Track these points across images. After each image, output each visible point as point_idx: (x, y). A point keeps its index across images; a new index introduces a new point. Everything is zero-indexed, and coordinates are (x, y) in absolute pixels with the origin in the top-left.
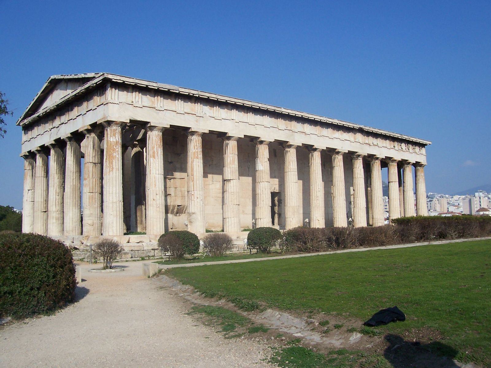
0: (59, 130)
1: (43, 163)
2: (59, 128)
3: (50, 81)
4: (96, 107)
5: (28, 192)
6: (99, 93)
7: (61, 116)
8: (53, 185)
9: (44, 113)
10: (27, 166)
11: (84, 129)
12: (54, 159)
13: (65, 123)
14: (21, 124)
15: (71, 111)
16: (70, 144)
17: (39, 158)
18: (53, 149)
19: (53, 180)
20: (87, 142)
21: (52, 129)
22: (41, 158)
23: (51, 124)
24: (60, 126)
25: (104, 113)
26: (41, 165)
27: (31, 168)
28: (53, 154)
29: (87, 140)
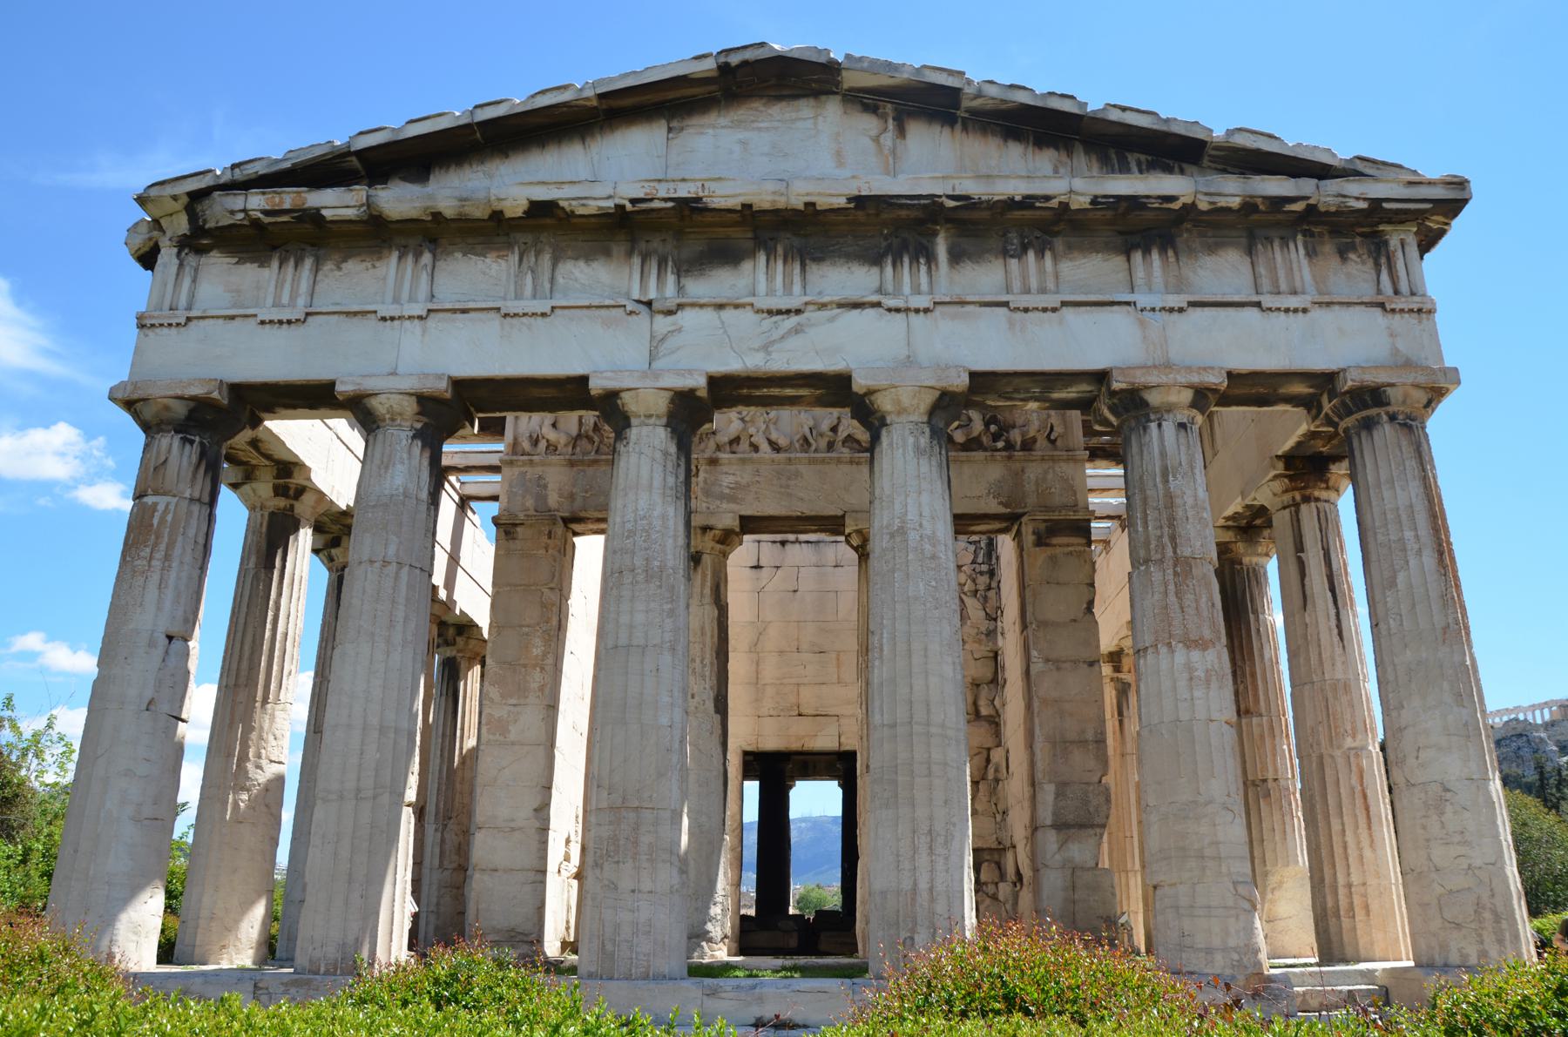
0: (797, 330)
2: (793, 320)
3: (745, 63)
4: (1308, 306)
5: (167, 652)
6: (1302, 251)
7: (818, 260)
8: (668, 636)
9: (656, 204)
10: (187, 472)
11: (1182, 379)
12: (671, 480)
13: (898, 310)
14: (257, 201)
15: (956, 257)
18: (664, 421)
20: (1183, 448)
21: (680, 306)
23: (671, 279)
24: (810, 315)
25: (1397, 350)
27: (206, 499)
28: (666, 454)
29: (1182, 440)
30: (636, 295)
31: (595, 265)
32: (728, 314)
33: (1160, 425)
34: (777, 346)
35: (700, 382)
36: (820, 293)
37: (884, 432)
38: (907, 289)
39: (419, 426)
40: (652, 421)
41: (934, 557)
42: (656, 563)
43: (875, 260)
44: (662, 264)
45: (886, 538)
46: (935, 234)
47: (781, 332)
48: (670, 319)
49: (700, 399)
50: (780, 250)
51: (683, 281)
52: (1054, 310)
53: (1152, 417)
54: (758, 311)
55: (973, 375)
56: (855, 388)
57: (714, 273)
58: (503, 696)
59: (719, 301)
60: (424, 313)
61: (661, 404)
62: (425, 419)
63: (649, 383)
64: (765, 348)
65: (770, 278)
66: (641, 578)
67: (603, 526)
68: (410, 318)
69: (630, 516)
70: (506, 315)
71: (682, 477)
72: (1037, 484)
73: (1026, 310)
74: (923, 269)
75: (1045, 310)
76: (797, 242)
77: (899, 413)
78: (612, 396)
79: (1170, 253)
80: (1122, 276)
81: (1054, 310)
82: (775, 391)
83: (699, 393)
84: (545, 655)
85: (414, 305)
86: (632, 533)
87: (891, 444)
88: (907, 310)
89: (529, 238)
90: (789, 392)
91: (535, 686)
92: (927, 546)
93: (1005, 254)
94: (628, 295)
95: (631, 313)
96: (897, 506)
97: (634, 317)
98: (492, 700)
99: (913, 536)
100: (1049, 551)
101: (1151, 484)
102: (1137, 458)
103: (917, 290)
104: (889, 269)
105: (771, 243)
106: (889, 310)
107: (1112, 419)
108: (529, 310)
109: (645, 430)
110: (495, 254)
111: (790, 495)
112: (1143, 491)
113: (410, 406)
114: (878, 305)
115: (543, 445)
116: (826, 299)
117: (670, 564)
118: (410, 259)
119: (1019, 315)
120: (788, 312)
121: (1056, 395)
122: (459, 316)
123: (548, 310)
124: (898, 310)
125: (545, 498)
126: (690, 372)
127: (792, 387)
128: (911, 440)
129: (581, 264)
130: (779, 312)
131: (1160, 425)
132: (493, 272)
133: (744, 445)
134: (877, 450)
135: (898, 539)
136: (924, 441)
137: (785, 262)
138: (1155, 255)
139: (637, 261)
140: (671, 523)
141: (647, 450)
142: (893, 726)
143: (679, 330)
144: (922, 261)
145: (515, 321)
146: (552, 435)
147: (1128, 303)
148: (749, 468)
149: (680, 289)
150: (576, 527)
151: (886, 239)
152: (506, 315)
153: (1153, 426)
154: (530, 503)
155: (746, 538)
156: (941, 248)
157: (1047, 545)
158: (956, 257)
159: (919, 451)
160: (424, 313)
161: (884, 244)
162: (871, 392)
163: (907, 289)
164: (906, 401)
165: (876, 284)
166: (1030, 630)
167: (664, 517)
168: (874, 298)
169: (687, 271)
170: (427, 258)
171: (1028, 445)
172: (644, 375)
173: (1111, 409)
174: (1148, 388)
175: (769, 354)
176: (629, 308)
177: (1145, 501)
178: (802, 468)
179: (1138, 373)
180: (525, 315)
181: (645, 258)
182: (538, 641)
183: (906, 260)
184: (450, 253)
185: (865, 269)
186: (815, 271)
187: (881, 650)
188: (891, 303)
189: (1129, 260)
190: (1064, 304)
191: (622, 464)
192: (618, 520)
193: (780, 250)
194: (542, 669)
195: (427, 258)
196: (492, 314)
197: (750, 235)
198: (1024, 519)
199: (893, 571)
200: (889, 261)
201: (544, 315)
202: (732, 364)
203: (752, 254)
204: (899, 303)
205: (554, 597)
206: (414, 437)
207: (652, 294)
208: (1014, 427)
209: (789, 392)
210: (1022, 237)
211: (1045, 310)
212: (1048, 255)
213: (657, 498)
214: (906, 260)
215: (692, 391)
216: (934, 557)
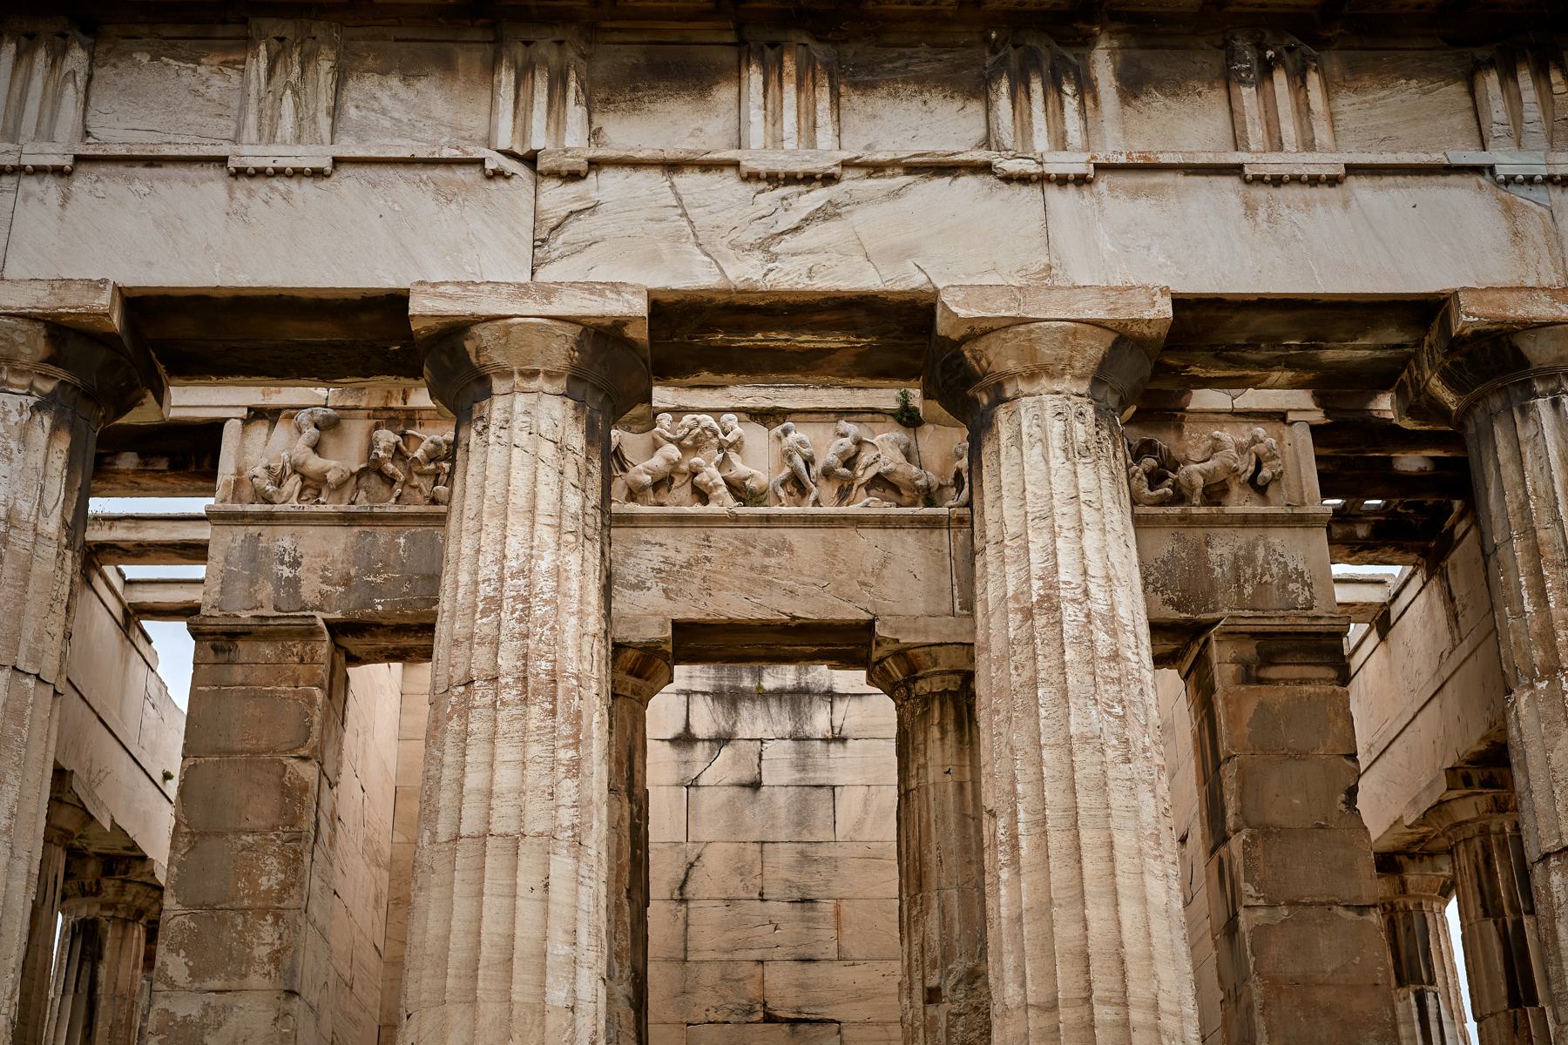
0: (827, 213)
1: (69, 519)
2: (819, 196)
8: (566, 817)
13: (1024, 179)
15: (1132, 86)
16: (1097, 411)
17: (40, 435)
18: (561, 385)
19: (565, 755)
21: (595, 164)
22: (63, 443)
23: (575, 113)
24: (854, 185)
26: (52, 526)
28: (561, 447)
30: (505, 140)
31: (422, 85)
32: (688, 181)
33: (1556, 404)
34: (790, 242)
35: (640, 307)
36: (868, 147)
37: (1001, 413)
38: (1041, 142)
39: (48, 387)
40: (540, 382)
41: (1115, 657)
42: (544, 665)
43: (980, 90)
44: (558, 85)
45: (1015, 619)
46: (1088, 42)
47: (793, 219)
48: (573, 188)
49: (631, 344)
50: (790, 66)
51: (596, 118)
52: (1333, 181)
53: (1539, 388)
54: (752, 177)
55: (1181, 303)
56: (943, 327)
57: (658, 106)
58: (194, 974)
59: (671, 154)
60: (67, 162)
61: (559, 351)
62: (62, 375)
63: (531, 307)
64: (763, 245)
65: (774, 117)
66: (511, 695)
67: (408, 641)
68: (39, 171)
69: (488, 570)
70: (240, 173)
71: (595, 498)
72: (1236, 568)
73: (1277, 181)
74: (1071, 104)
75: (1314, 181)
76: (819, 51)
77: (1032, 377)
78: (455, 331)
79: (1556, 77)
80: (1461, 120)
81: (1333, 181)
82: (779, 339)
83: (631, 332)
84: (285, 887)
85: (47, 147)
86: (494, 604)
87: (1018, 436)
88: (1043, 179)
89: (288, 29)
90: (806, 340)
91: (262, 952)
92: (1101, 637)
93: (1228, 79)
94: (488, 142)
95: (498, 174)
96: (1036, 557)
97: (502, 183)
98: (171, 984)
99: (1070, 612)
100: (1266, 692)
101: (1546, 518)
102: (1509, 471)
103: (1061, 142)
104: (1003, 104)
105: (769, 53)
106: (1008, 179)
107: (1448, 398)
108: (289, 164)
109: (520, 402)
110: (217, 60)
111: (769, 584)
112: (1529, 531)
113: (33, 346)
114: (986, 168)
115: (293, 484)
116: (880, 157)
117: (572, 668)
118: (41, 59)
119: (1260, 193)
120: (809, 179)
121: (1329, 355)
122: (140, 171)
123: (326, 164)
124: (1024, 179)
125: (294, 583)
126: (616, 287)
127: (816, 328)
128: (1057, 427)
129: (394, 82)
130: (791, 179)
131: (1556, 404)
132: (213, 93)
133: (682, 491)
134: (987, 450)
135: (1040, 621)
136: (1081, 432)
137: (799, 87)
138: (1525, 80)
139: (506, 78)
140: (574, 586)
141: (526, 451)
142: (1052, 1007)
143: (592, 209)
144: (1068, 89)
145: (258, 185)
146: (315, 463)
147: (1477, 170)
148: (692, 535)
149: (595, 135)
150: (354, 644)
151: (994, 51)
152: (240, 173)
153: (1543, 406)
154: (266, 591)
155: (680, 671)
156: (1103, 67)
157: (1260, 681)
158: (1132, 86)
159: (1071, 451)
160: (67, 162)
161: (989, 61)
162: (980, 331)
163: (1041, 142)
164: (1047, 352)
165: (980, 132)
166: (1236, 844)
167: (558, 573)
168: (980, 156)
169: (607, 101)
170: (77, 59)
171: (1215, 492)
172: (522, 290)
173: (1448, 379)
174: (1532, 327)
175: (774, 257)
176: (489, 166)
177: (1536, 552)
178: (793, 535)
179: (1511, 298)
180: (279, 172)
181: (523, 75)
182: (272, 863)
183: (1037, 86)
184: (127, 54)
185: (958, 104)
186: (853, 100)
187: (1015, 847)
188: (1013, 166)
189: (1472, 92)
190: (1353, 169)
191: (473, 468)
192: (464, 578)
193: (790, 66)
194: (277, 917)
195: (77, 59)
196: (211, 171)
197: (730, 37)
198: (1212, 633)
199: (1034, 684)
200: (1004, 86)
201: (317, 173)
202: (695, 274)
203: (736, 75)
204: (1031, 168)
205: (309, 772)
206: (37, 408)
207: (539, 140)
208: (1186, 461)
209: (806, 340)
210: (1260, 47)
211: (1314, 181)
212: (1314, 80)
213: (546, 534)
214: (1037, 86)
215: (619, 324)
216: (1115, 657)
